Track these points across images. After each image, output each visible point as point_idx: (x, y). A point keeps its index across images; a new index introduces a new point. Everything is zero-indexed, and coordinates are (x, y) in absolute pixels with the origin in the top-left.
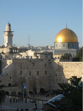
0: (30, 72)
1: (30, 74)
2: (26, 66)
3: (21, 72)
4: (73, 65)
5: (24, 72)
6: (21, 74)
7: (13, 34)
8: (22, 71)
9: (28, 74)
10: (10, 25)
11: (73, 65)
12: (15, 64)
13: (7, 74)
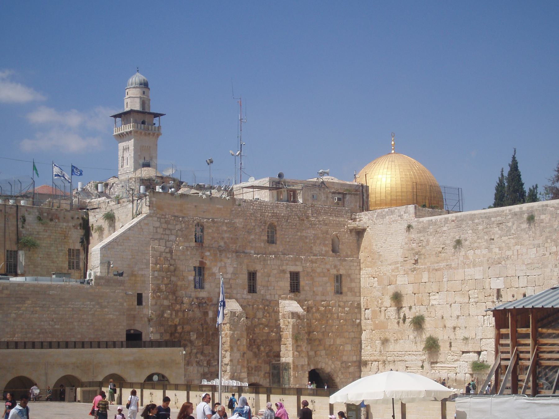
0: (252, 276)
1: (252, 289)
2: (226, 235)
3: (200, 270)
4: (499, 224)
5: (215, 270)
6: (199, 285)
7: (159, 127)
8: (208, 263)
9: (239, 281)
10: (145, 85)
11: (499, 224)
12: (167, 223)
13: (121, 275)
